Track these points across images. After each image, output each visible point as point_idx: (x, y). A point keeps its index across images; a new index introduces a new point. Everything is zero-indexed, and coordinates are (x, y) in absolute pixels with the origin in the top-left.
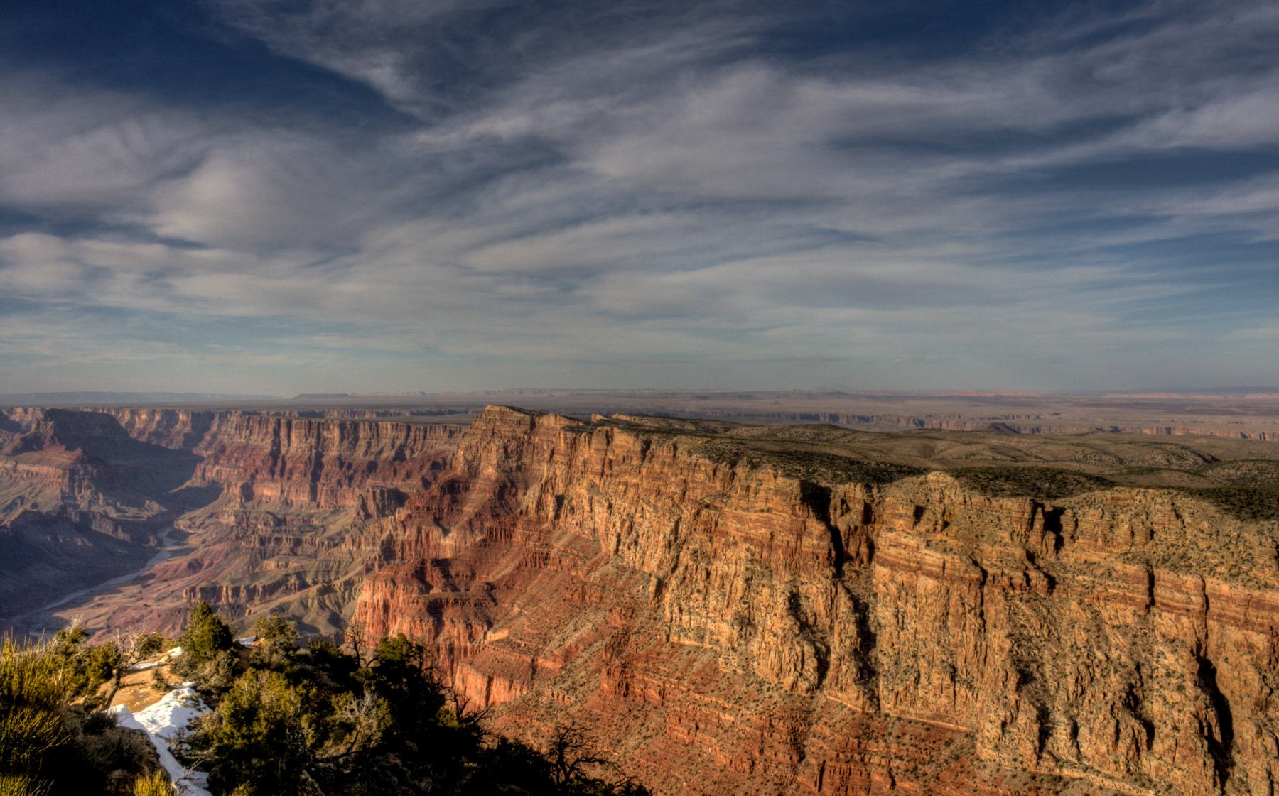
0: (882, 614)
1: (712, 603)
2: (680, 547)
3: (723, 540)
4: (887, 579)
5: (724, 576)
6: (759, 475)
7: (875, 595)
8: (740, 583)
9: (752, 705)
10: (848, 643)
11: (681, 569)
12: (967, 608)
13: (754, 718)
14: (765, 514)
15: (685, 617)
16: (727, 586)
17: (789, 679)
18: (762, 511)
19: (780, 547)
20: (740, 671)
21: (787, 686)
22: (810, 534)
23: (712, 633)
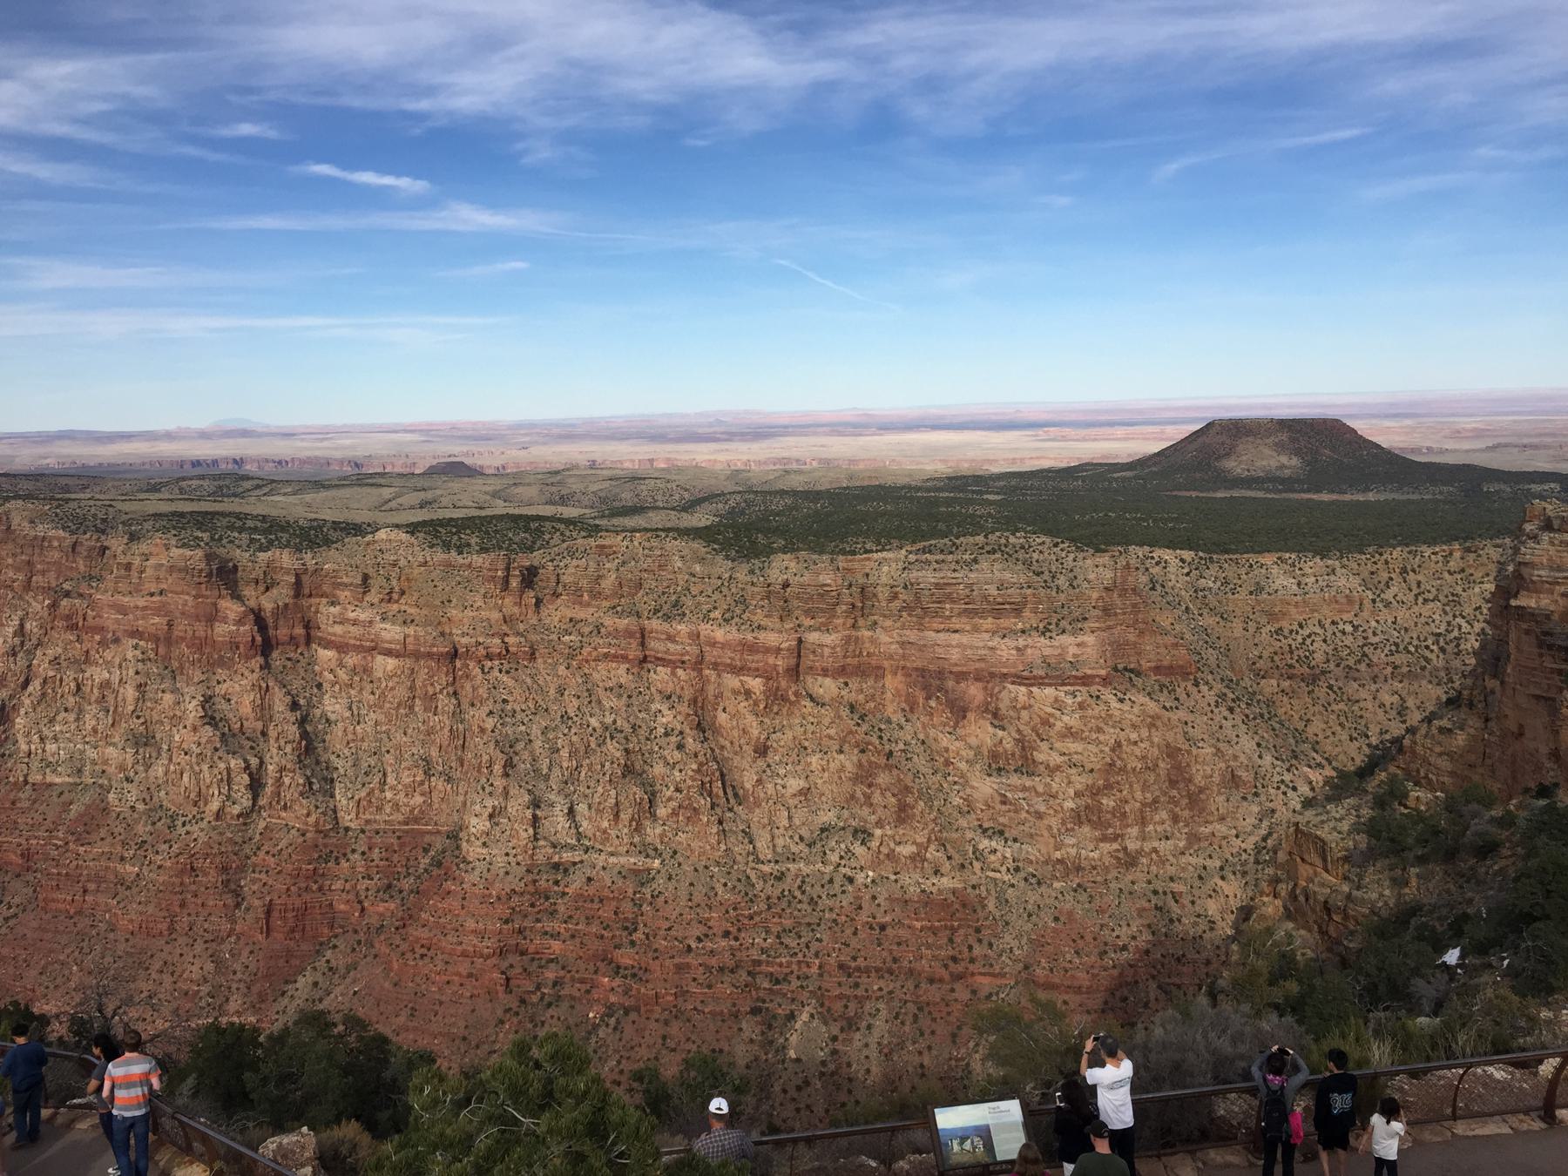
0: (333, 706)
1: (90, 723)
2: (31, 653)
3: (97, 638)
4: (333, 664)
5: (106, 685)
6: (144, 547)
7: (319, 686)
8: (130, 693)
9: (166, 847)
10: (288, 749)
11: (35, 686)
12: (438, 688)
13: (168, 864)
14: (155, 599)
15: (51, 747)
16: (111, 698)
17: (215, 805)
18: (152, 595)
19: (183, 639)
20: (140, 807)
21: (209, 816)
22: (225, 620)
23: (94, 763)
